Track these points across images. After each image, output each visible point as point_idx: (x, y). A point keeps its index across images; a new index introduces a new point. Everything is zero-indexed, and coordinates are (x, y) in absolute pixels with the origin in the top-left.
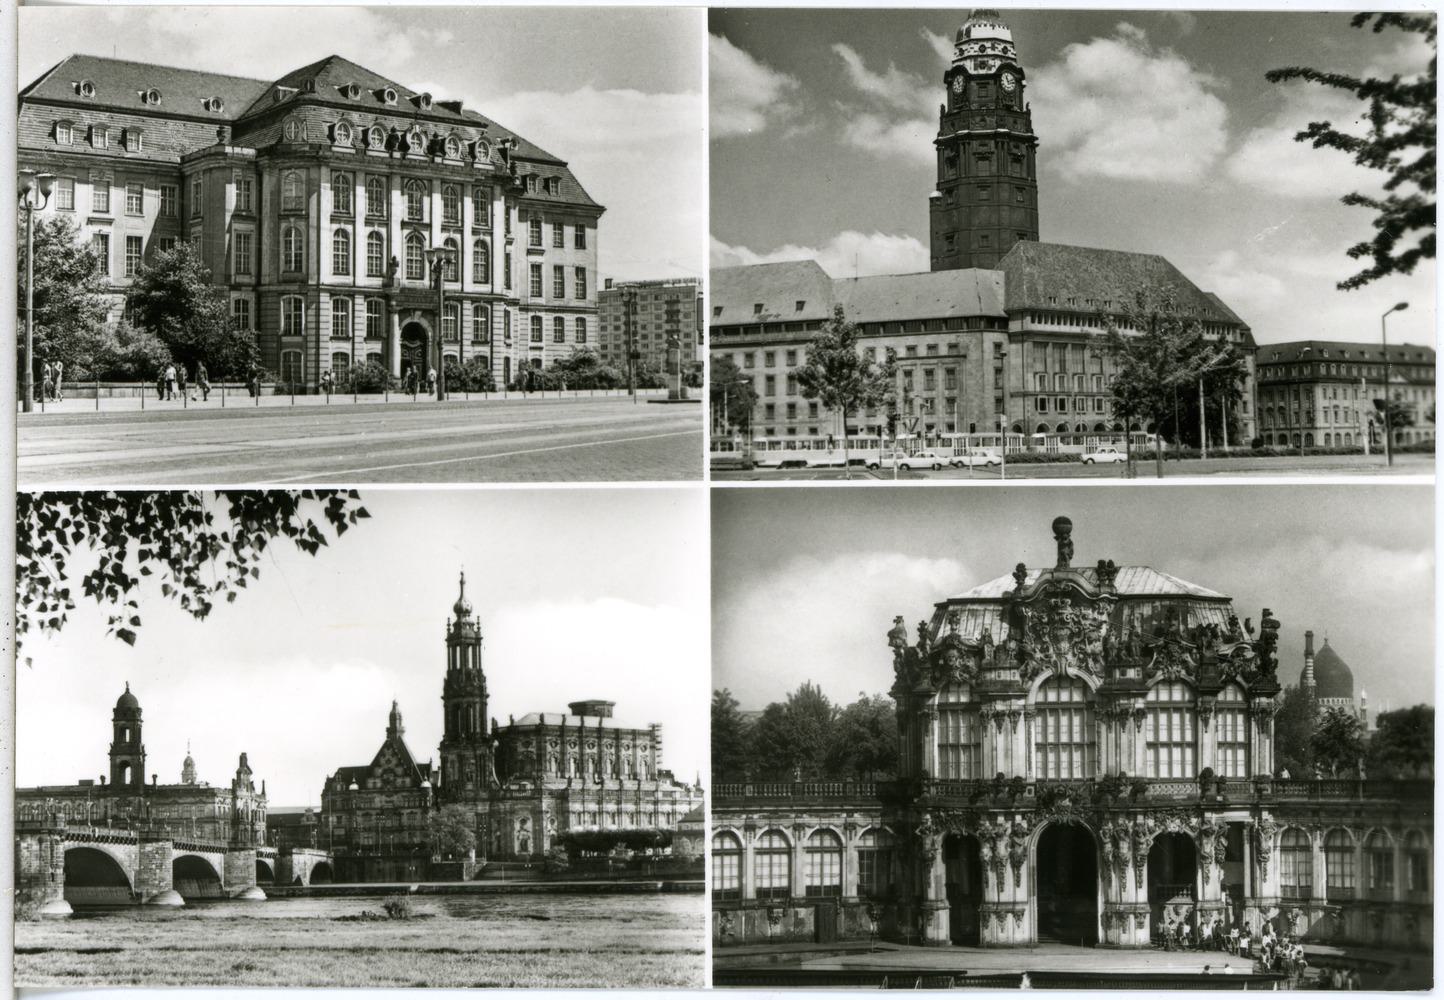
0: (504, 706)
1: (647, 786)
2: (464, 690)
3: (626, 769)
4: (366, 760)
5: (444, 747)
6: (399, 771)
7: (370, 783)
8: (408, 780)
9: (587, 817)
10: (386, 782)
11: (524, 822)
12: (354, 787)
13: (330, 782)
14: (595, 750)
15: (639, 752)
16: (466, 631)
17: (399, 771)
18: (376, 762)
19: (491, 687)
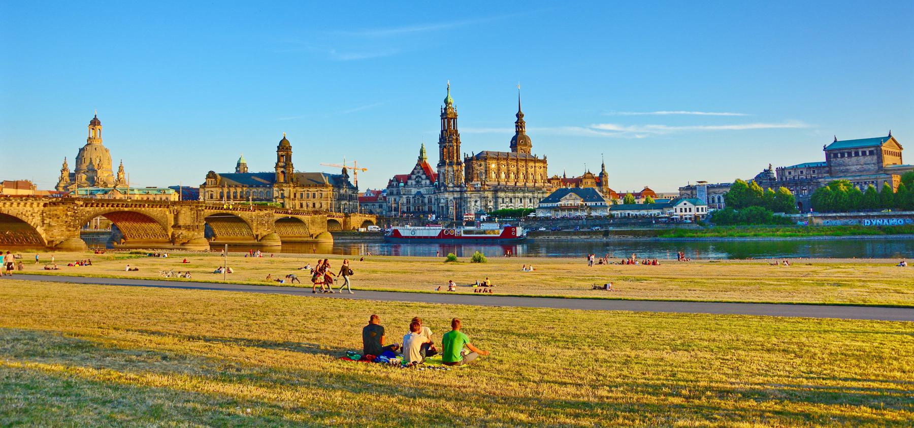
0: (467, 148)
1: (539, 184)
2: (448, 138)
3: (531, 177)
4: (409, 172)
5: (439, 166)
6: (424, 177)
7: (410, 182)
8: (428, 182)
9: (508, 200)
10: (418, 182)
11: (476, 202)
12: (402, 184)
13: (391, 181)
14: (515, 169)
15: (537, 169)
16: (449, 111)
17: (424, 177)
18: (413, 173)
19: (461, 139)
